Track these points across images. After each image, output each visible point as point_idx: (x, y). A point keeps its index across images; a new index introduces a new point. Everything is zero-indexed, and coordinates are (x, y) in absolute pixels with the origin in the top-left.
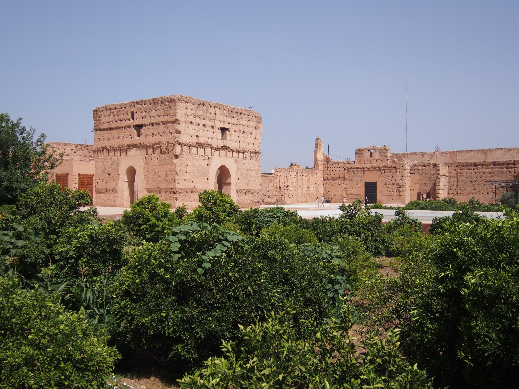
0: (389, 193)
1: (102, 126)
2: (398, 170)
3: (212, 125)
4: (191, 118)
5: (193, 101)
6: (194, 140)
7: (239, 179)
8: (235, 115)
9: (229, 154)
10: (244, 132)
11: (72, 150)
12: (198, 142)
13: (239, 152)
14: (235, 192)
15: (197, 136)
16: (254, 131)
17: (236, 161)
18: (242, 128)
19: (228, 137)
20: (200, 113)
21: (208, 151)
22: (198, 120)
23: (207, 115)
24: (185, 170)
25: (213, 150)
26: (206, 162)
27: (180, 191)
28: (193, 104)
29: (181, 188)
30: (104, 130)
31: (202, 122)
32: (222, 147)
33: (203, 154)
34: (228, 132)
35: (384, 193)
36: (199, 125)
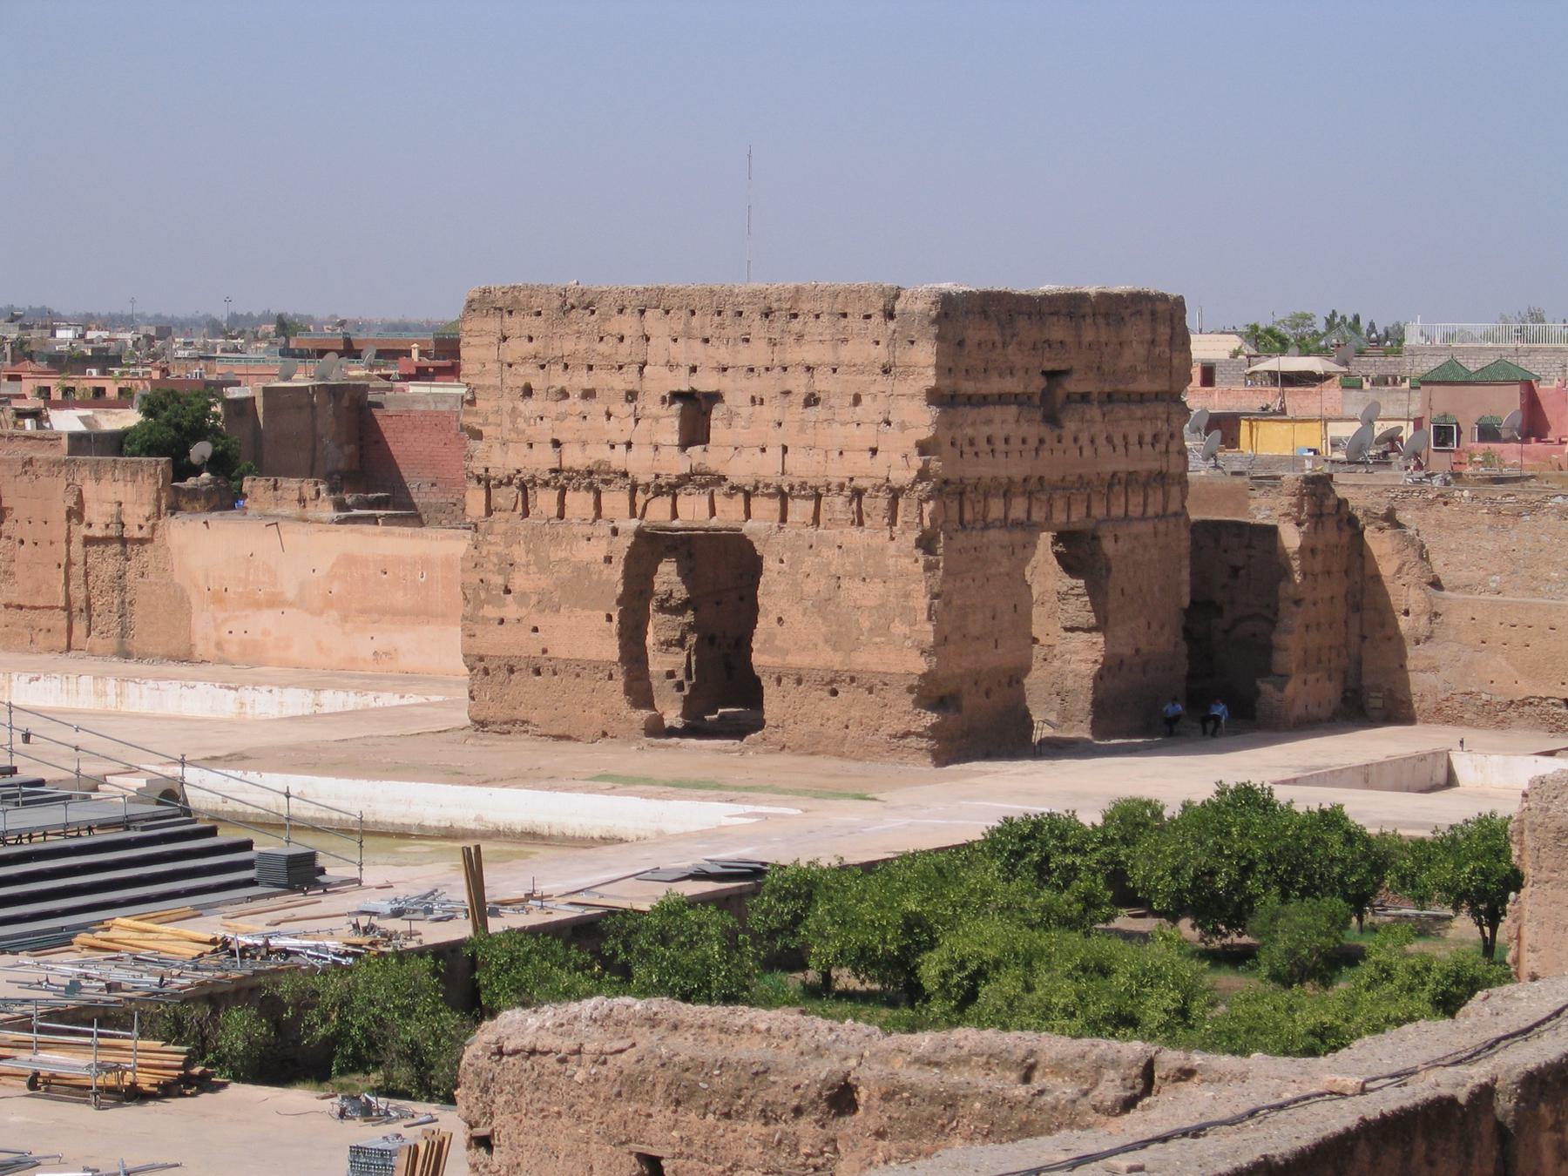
3: (630, 387)
4: (529, 373)
5: (536, 303)
6: (542, 460)
8: (757, 326)
10: (812, 400)
13: (783, 496)
15: (557, 444)
16: (883, 383)
19: (718, 429)
20: (568, 346)
22: (559, 380)
23: (601, 347)
24: (498, 580)
25: (639, 493)
27: (481, 665)
28: (539, 314)
29: (482, 652)
34: (717, 412)
36: (564, 394)
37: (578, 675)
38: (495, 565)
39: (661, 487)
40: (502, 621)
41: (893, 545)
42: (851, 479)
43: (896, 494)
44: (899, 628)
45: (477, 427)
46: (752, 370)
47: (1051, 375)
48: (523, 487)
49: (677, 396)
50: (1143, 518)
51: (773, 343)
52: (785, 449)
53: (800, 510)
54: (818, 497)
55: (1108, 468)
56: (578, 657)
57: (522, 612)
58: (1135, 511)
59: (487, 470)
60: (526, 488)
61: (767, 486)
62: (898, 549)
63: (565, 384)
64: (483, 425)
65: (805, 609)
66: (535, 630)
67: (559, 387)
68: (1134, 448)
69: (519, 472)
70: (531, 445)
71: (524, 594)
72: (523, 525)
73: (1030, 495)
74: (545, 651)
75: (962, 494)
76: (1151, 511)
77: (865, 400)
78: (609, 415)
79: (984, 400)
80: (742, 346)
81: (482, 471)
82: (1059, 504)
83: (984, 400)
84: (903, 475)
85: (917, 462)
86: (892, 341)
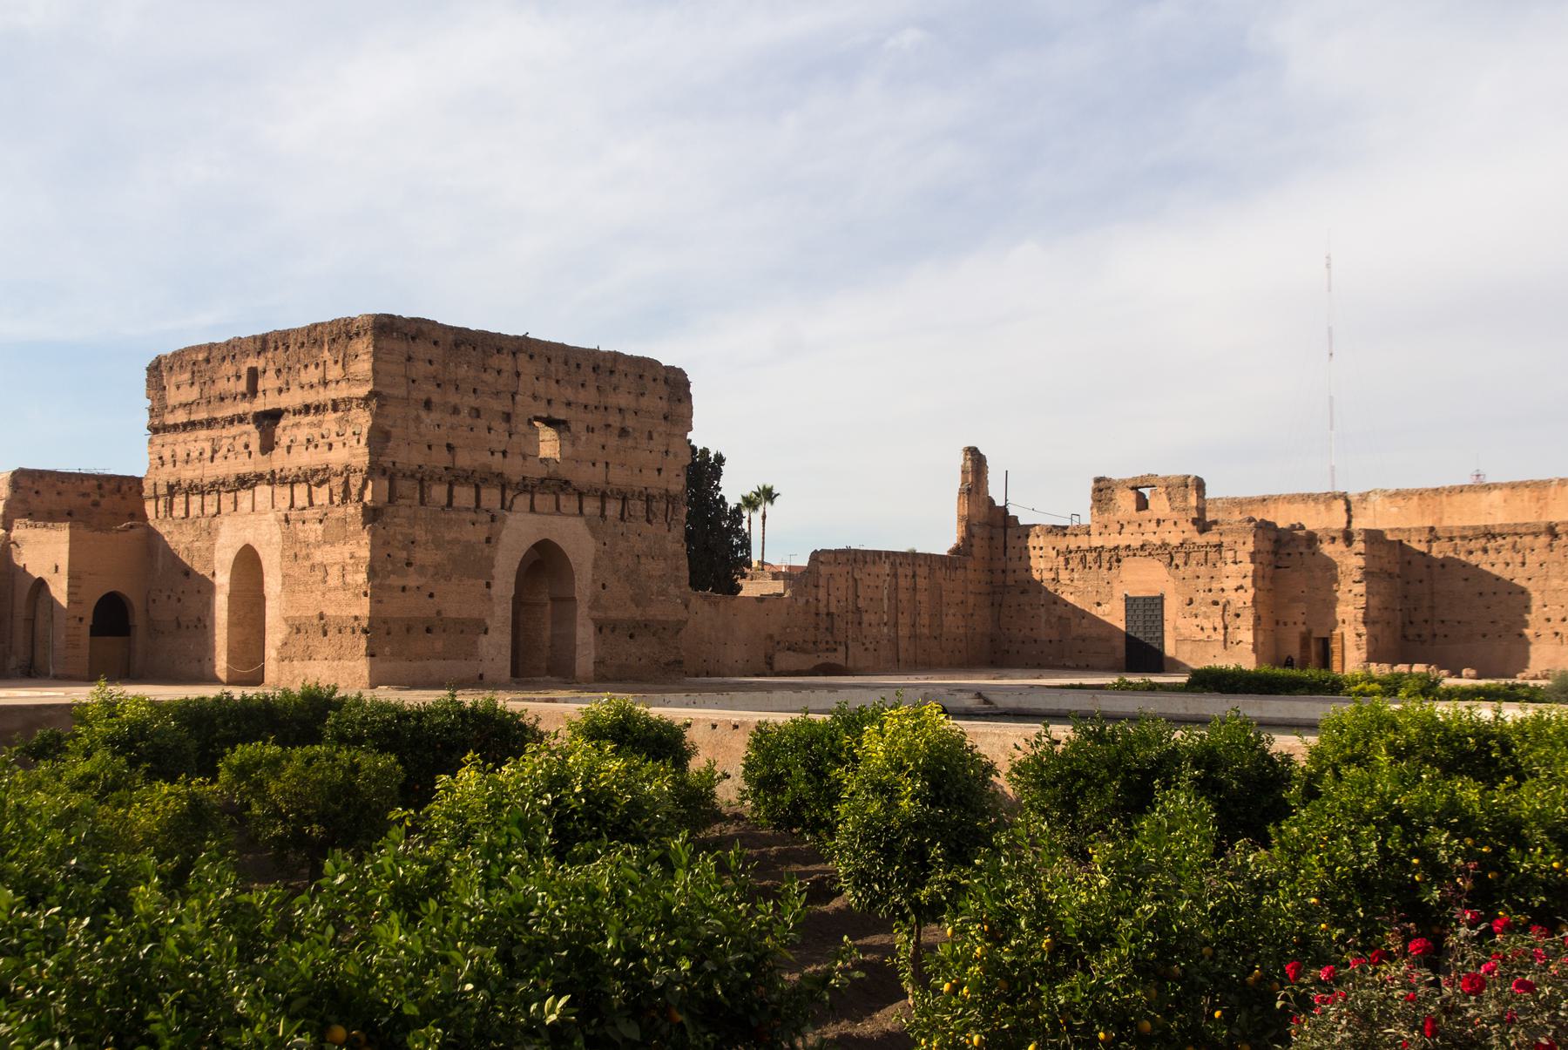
0: (1203, 636)
1: (170, 419)
2: (1229, 555)
3: (506, 409)
4: (429, 390)
6: (440, 458)
7: (604, 586)
10: (623, 432)
11: (84, 495)
12: (451, 465)
14: (591, 629)
15: (450, 447)
16: (662, 427)
17: (593, 531)
18: (615, 420)
21: (491, 497)
22: (454, 399)
23: (485, 377)
24: (404, 554)
26: (481, 532)
28: (436, 343)
30: (175, 427)
31: (471, 400)
32: (543, 480)
33: (473, 505)
35: (1186, 633)
37: (462, 632)
38: (400, 542)
39: (526, 486)
40: (404, 589)
41: (670, 536)
42: (646, 489)
44: (672, 590)
45: (388, 428)
46: (586, 407)
48: (422, 480)
53: (613, 508)
54: (624, 499)
56: (465, 616)
57: (422, 581)
59: (394, 463)
60: (422, 479)
62: (673, 538)
63: (458, 401)
64: (392, 427)
65: (619, 578)
66: (431, 595)
67: (453, 403)
69: (420, 467)
70: (430, 447)
71: (423, 566)
72: (422, 512)
74: (439, 613)
77: (655, 435)
78: (490, 429)
80: (581, 390)
81: (391, 465)
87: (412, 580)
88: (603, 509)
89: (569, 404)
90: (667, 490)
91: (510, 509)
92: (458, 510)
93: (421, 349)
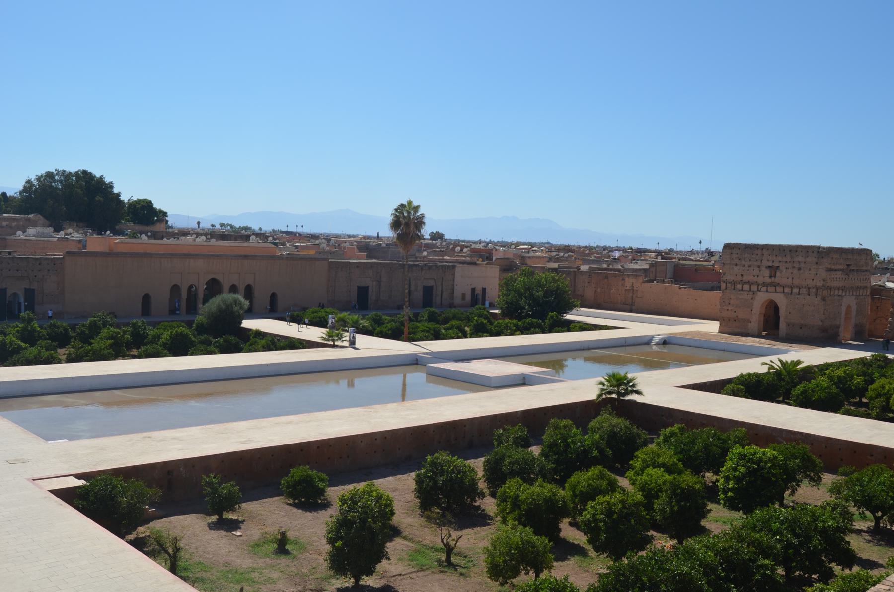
6: (740, 278)
7: (790, 313)
9: (781, 289)
10: (800, 269)
18: (796, 265)
19: (778, 274)
21: (754, 288)
22: (743, 263)
23: (753, 256)
24: (728, 301)
26: (750, 296)
31: (747, 263)
33: (749, 290)
40: (728, 310)
41: (816, 299)
43: (817, 288)
47: (848, 265)
49: (769, 267)
50: (862, 295)
51: (792, 257)
52: (793, 278)
53: (795, 290)
54: (800, 288)
55: (857, 285)
58: (861, 294)
60: (734, 283)
61: (789, 286)
66: (735, 312)
68: (862, 281)
70: (736, 275)
73: (843, 289)
74: (737, 317)
75: (831, 289)
76: (864, 294)
78: (754, 270)
79: (836, 270)
82: (848, 292)
83: (836, 270)
84: (820, 284)
85: (822, 282)
86: (818, 258)
87: (730, 308)
88: (792, 291)
89: (780, 262)
90: (816, 285)
91: (760, 291)
92: (744, 290)
93: (735, 251)
